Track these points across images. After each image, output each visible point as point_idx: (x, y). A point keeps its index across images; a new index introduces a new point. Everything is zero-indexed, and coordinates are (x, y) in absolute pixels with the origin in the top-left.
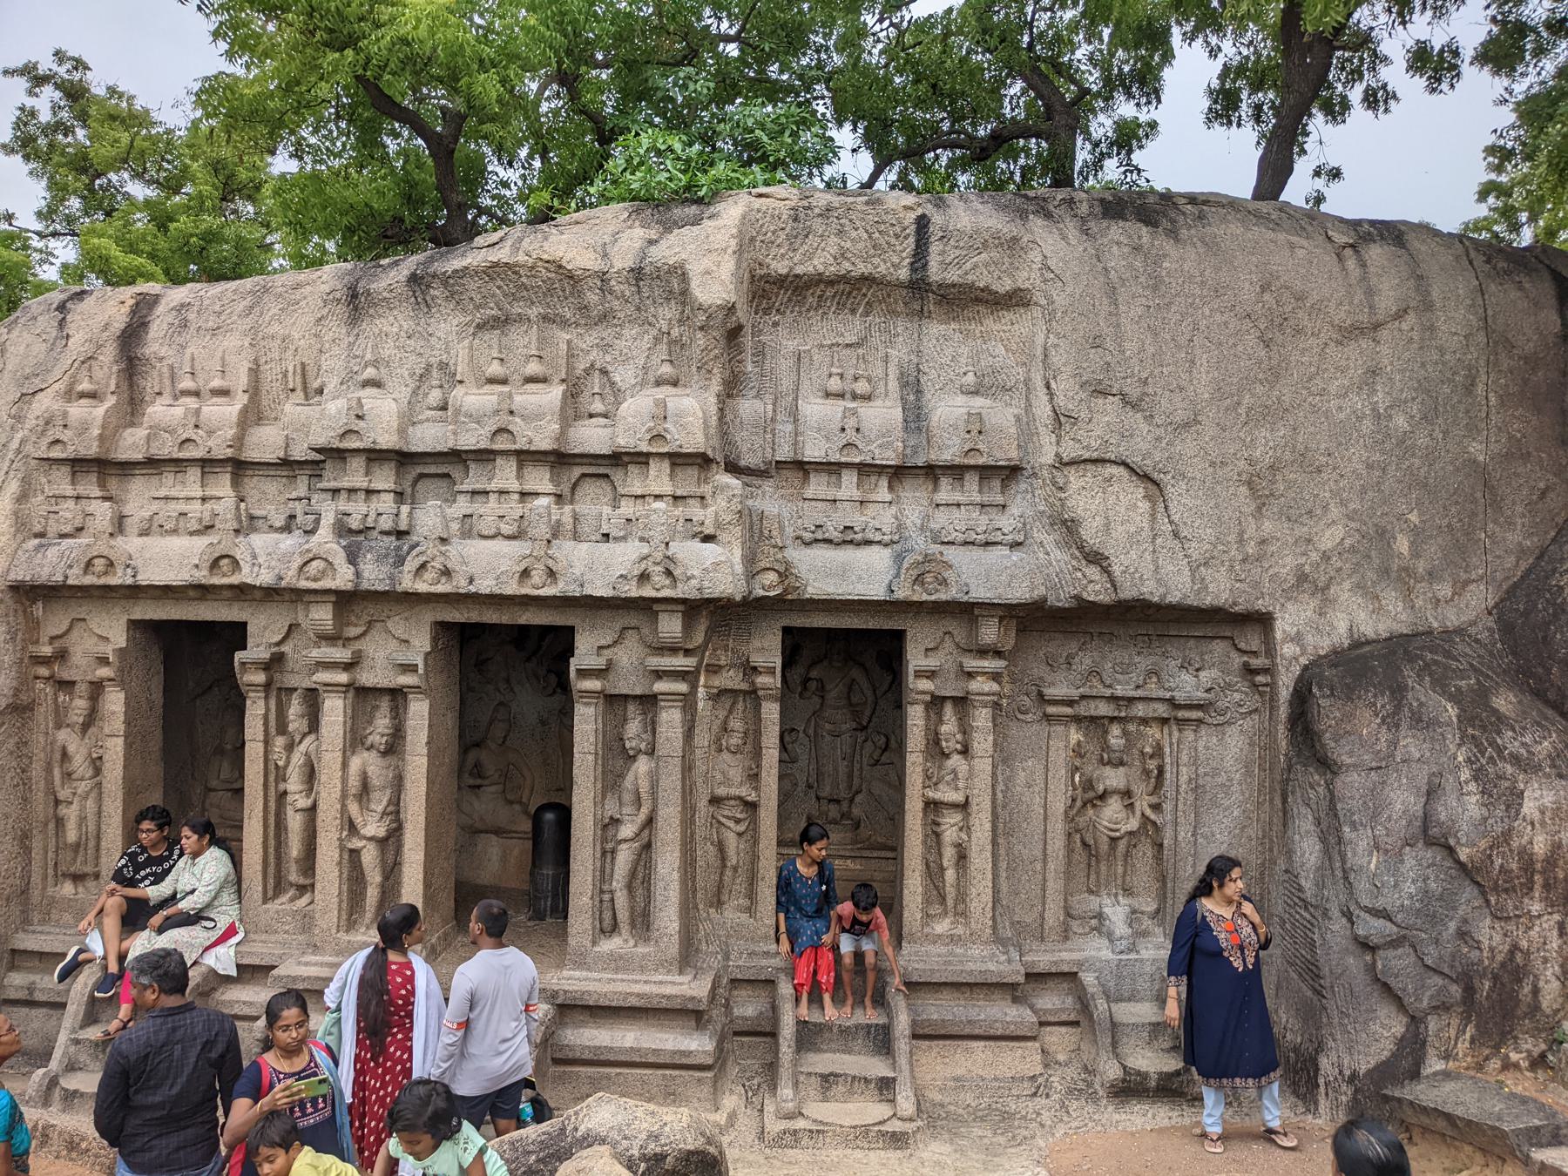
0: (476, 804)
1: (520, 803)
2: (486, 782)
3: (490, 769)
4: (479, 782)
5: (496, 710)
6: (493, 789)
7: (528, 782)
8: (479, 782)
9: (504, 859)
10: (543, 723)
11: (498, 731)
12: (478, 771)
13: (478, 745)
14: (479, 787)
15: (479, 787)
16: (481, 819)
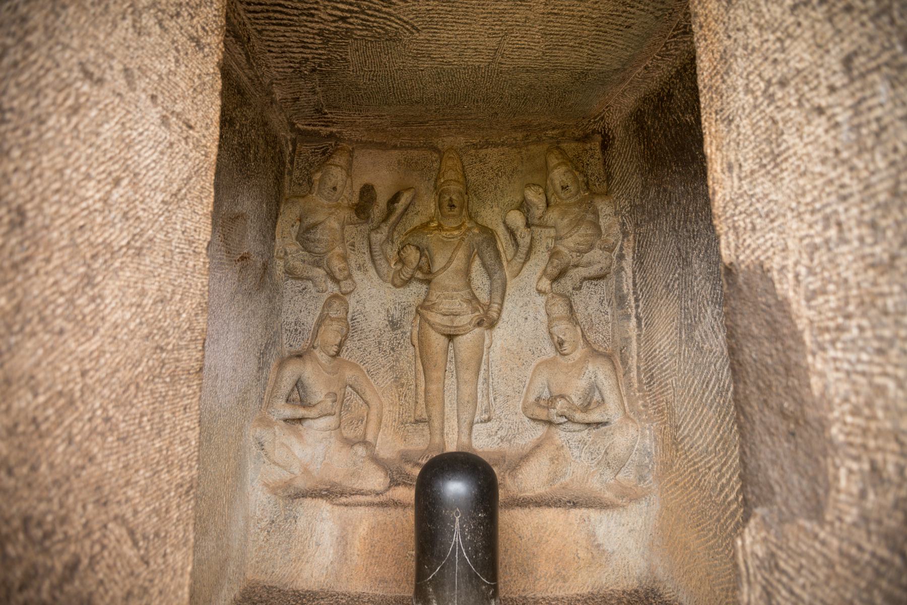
0: (297, 449)
1: (364, 443)
2: (313, 413)
3: (319, 391)
4: (301, 412)
5: (328, 304)
6: (323, 422)
7: (374, 411)
8: (301, 412)
9: (343, 541)
10: (394, 325)
11: (331, 335)
12: (299, 394)
13: (299, 356)
14: (300, 420)
15: (300, 420)
16: (306, 471)
